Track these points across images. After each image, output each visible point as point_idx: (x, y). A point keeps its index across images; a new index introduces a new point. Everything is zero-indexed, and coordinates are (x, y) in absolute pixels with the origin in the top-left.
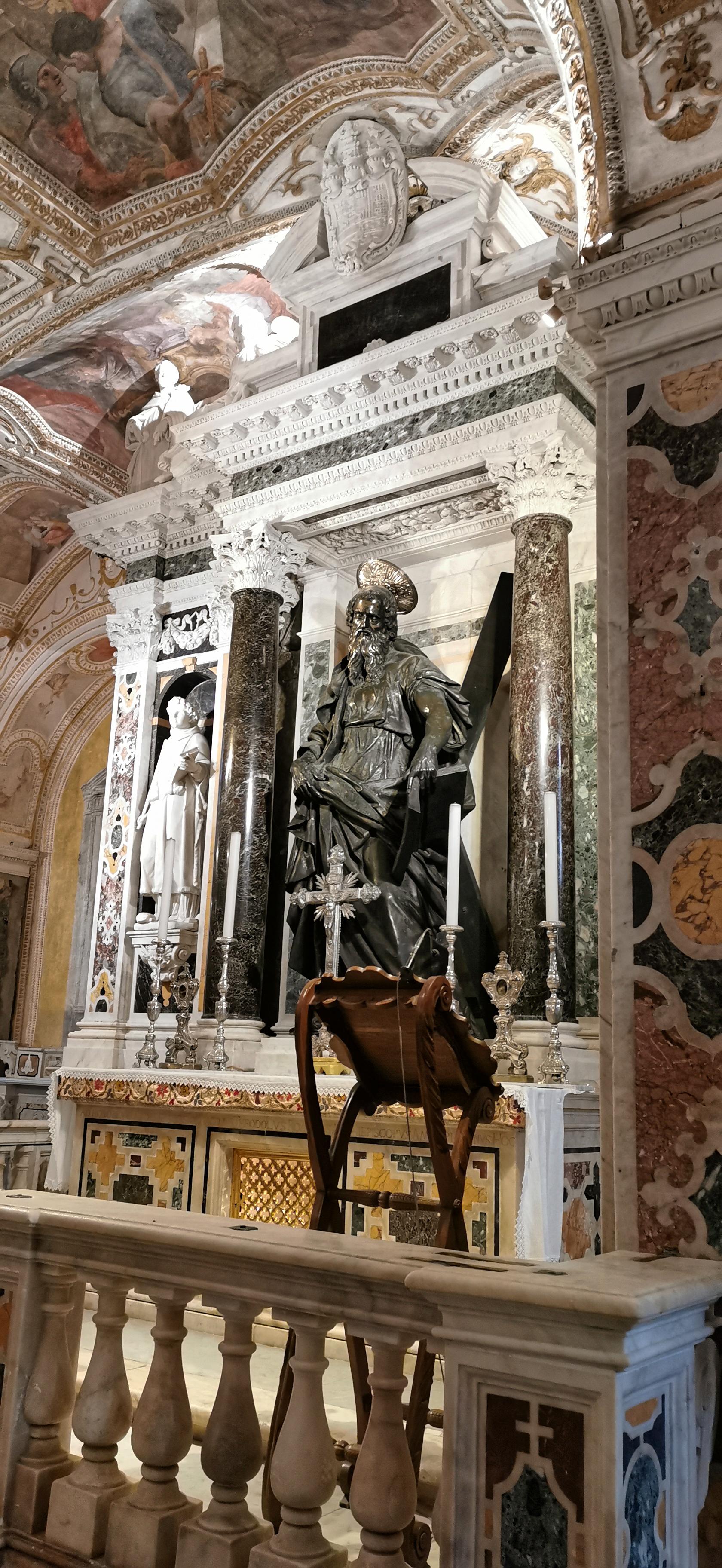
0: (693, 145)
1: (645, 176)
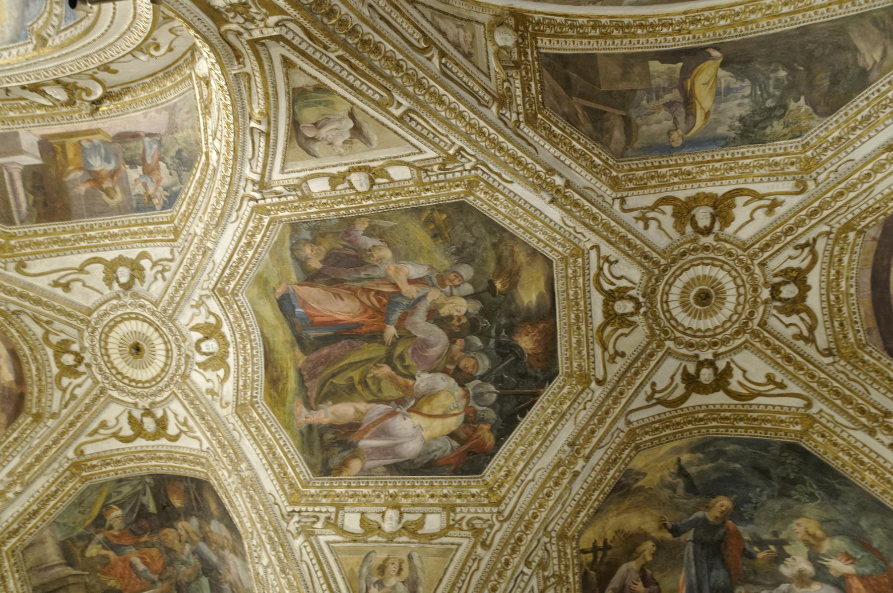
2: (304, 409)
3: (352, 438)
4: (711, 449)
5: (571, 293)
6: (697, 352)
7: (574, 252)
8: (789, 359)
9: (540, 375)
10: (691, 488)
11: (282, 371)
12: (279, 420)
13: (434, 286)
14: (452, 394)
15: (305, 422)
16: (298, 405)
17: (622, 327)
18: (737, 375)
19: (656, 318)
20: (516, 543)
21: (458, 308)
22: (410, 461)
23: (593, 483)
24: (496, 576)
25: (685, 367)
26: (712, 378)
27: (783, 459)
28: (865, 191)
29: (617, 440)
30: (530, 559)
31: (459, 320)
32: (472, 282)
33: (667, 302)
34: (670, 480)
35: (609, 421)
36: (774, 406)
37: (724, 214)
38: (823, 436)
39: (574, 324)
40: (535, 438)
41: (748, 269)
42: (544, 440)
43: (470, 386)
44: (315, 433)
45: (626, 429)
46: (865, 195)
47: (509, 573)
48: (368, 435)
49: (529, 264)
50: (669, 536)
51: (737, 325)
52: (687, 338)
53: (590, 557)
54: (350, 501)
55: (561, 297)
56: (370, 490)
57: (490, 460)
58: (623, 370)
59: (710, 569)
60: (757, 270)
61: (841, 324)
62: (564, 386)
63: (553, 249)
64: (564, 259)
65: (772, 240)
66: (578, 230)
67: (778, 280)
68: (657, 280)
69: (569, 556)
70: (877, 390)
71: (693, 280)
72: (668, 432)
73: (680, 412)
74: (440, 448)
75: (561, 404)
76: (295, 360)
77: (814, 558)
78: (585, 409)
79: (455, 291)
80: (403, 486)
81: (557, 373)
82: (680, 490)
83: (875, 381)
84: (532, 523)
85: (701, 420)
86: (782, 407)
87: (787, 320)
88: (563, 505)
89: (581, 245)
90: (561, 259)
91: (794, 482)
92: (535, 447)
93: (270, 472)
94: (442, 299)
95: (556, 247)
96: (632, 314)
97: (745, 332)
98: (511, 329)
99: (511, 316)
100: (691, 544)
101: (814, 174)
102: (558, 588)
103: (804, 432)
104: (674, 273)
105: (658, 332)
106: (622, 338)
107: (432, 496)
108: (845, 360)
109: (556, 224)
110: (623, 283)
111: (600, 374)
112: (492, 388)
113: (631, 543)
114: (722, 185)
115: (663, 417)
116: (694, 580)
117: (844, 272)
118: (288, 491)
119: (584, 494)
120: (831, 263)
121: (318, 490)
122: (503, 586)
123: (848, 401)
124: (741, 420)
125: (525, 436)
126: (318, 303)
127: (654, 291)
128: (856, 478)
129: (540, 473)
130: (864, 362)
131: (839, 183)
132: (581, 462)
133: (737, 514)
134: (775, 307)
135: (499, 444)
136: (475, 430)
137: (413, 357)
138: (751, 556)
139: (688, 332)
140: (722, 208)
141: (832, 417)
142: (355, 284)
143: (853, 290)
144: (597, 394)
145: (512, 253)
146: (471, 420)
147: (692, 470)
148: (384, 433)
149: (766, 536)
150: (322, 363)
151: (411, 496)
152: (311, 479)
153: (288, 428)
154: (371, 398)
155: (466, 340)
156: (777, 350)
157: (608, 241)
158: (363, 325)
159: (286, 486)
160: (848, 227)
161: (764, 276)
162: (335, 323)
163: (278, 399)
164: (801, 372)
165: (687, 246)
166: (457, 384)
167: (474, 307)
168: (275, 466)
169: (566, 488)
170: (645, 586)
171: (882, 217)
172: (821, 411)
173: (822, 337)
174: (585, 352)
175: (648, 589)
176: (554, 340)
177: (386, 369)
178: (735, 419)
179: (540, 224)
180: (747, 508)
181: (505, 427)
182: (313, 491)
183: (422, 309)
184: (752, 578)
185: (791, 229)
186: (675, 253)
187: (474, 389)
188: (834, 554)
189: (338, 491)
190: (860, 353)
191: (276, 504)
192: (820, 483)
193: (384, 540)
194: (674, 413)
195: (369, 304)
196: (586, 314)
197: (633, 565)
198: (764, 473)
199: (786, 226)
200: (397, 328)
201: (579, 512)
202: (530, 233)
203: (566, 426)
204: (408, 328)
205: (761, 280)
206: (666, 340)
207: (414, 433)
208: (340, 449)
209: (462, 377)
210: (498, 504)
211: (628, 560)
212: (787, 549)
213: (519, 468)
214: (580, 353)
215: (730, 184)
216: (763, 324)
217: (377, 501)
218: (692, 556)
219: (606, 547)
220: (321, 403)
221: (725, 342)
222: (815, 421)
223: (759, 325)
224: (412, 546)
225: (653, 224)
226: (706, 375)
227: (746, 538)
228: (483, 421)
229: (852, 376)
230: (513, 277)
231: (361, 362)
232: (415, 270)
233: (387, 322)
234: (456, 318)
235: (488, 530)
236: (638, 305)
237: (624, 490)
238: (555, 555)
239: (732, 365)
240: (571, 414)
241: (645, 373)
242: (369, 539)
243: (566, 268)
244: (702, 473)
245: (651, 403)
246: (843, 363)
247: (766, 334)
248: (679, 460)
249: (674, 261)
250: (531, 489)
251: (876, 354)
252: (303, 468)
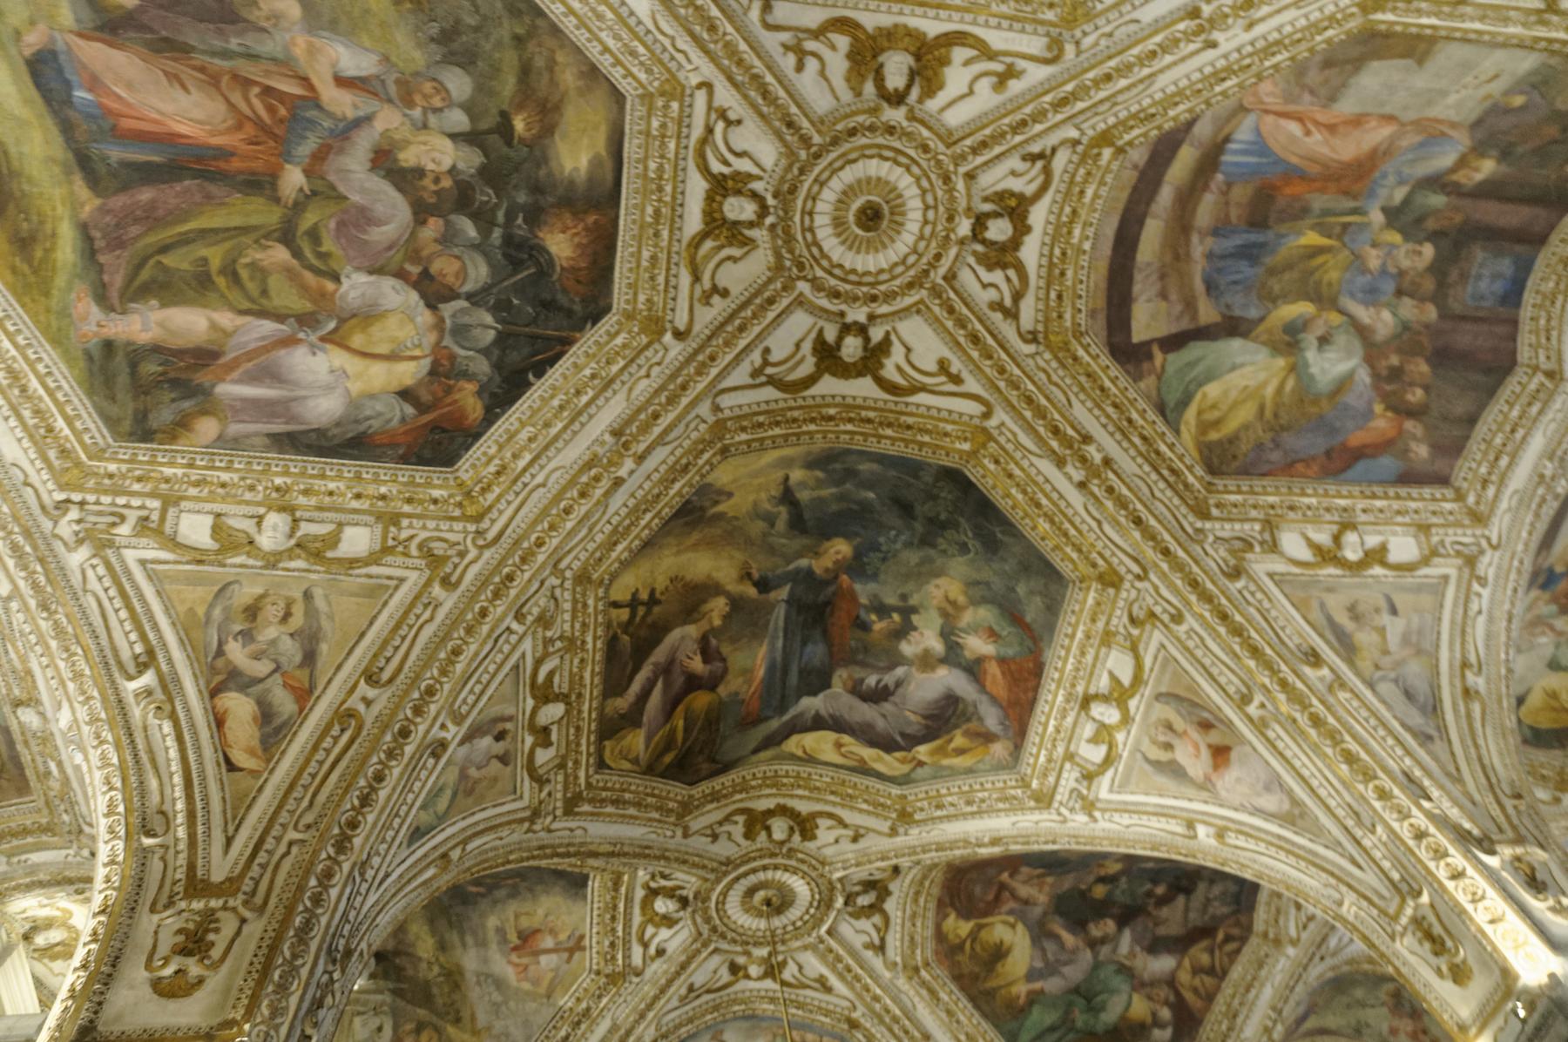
0: (172, 1005)
1: (118, 1018)
2: (95, 312)
3: (203, 378)
4: (838, 466)
5: (652, 165)
6: (843, 307)
7: (667, 87)
8: (975, 339)
9: (577, 308)
10: (798, 523)
11: (42, 223)
12: (37, 322)
13: (390, 101)
14: (412, 320)
15: (96, 334)
16: (79, 299)
17: (731, 245)
18: (897, 352)
19: (789, 239)
20: (502, 582)
21: (436, 155)
22: (320, 432)
23: (645, 500)
24: (462, 632)
25: (821, 331)
26: (859, 353)
27: (935, 491)
28: (1141, 81)
29: (694, 435)
30: (524, 610)
31: (437, 180)
32: (468, 108)
33: (811, 214)
34: (767, 506)
35: (685, 401)
36: (939, 410)
37: (930, 73)
38: (997, 462)
39: (650, 225)
40: (555, 416)
41: (947, 179)
42: (572, 421)
43: (447, 309)
44: (120, 360)
45: (711, 419)
46: (1141, 87)
47: (485, 629)
48: (235, 375)
49: (581, 92)
50: (752, 591)
51: (912, 273)
52: (833, 282)
53: (624, 614)
54: (193, 491)
55: (633, 171)
56: (236, 477)
57: (471, 445)
58: (720, 319)
59: (804, 643)
60: (960, 185)
61: (1060, 297)
62: (617, 333)
63: (629, 74)
64: (647, 97)
65: (992, 137)
66: (681, 44)
67: (988, 207)
68: (802, 171)
69: (591, 610)
70: (1083, 402)
71: (859, 181)
72: (777, 431)
73: (800, 402)
74: (380, 414)
75: (608, 363)
76: (75, 205)
77: (948, 634)
78: (648, 376)
79: (433, 120)
80: (303, 474)
81: (608, 309)
82: (781, 524)
83: (1083, 389)
84: (533, 554)
85: (831, 418)
86: (950, 412)
88: (590, 530)
89: (681, 75)
90: (642, 97)
91: (944, 526)
92: (554, 431)
93: (13, 422)
94: (405, 132)
95: (635, 70)
96: (751, 225)
97: (921, 286)
98: (535, 216)
99: (537, 189)
100: (783, 605)
101: (1078, 33)
102: (567, 657)
103: (974, 453)
104: (830, 164)
105: (788, 263)
106: (729, 264)
107: (358, 496)
108: (1052, 351)
109: (640, 23)
110: (744, 165)
111: (681, 321)
112: (489, 319)
113: (691, 598)
114: (937, 18)
115: (773, 406)
116: (779, 659)
117: (1083, 213)
118: (56, 463)
119: (628, 515)
120: (1068, 193)
121: (124, 467)
122: (473, 648)
123: (1041, 413)
124: (890, 425)
125: (539, 409)
126: (129, 86)
127: (793, 190)
128: (1025, 526)
129: (558, 473)
130: (1075, 359)
131: (1110, 58)
132: (629, 464)
133: (857, 567)
134: (975, 253)
135: (490, 418)
136: (449, 390)
137: (338, 238)
138: (865, 627)
139: (837, 271)
140: (929, 59)
141: (1014, 435)
142: (217, 61)
143: (1087, 246)
144: (672, 354)
145: (551, 65)
146: (443, 371)
147: (804, 496)
148: (269, 374)
149: (891, 600)
150: (136, 221)
151: (317, 493)
152: (109, 446)
153: (56, 342)
154: (246, 305)
155: (448, 223)
156: (961, 323)
157: (730, 79)
158: (233, 154)
159: (52, 454)
160: (1105, 138)
161: (969, 196)
162: (168, 140)
163: (32, 279)
164: (988, 362)
165: (860, 119)
166: (422, 303)
167: (469, 160)
168: (27, 414)
169: (598, 502)
170: (706, 661)
171: (1155, 132)
172: (1003, 424)
173: (1029, 311)
174: (661, 279)
175: (708, 667)
176: (611, 249)
177: (281, 254)
178: (881, 424)
179: (610, 15)
180: (874, 557)
181: (508, 387)
182: (112, 467)
183: (363, 144)
184: (860, 657)
185: (1024, 123)
186: (839, 127)
187: (454, 316)
188: (974, 629)
189: (168, 471)
190: (1075, 345)
191: (27, 484)
192: (979, 533)
193: (259, 564)
194: (793, 404)
195: (248, 112)
196: (673, 210)
197: (692, 631)
198: (906, 509)
199: (1018, 117)
200: (308, 173)
201: (615, 544)
202: (590, 31)
203: (612, 402)
204: (332, 178)
205: (962, 204)
206: (799, 278)
207: (327, 380)
208: (173, 395)
209: (433, 292)
210: (478, 518)
211: (685, 623)
212: (915, 619)
213: (521, 464)
214: (652, 278)
215: (950, 20)
216: (950, 277)
217: (248, 496)
218: (781, 623)
219: (653, 600)
220: (132, 300)
221: (890, 296)
222: (991, 438)
223: (945, 278)
224: (314, 576)
225: (812, 65)
226: (851, 348)
227: (863, 600)
228: (466, 375)
229: (1055, 378)
230: (548, 113)
231: (227, 230)
232: (354, 60)
233: (287, 156)
234: (430, 177)
235: (456, 560)
236: (764, 210)
237: (693, 515)
238: (567, 606)
239: (893, 337)
240: (623, 383)
241: (757, 330)
242: (229, 561)
243: (649, 116)
244: (820, 501)
245: (758, 381)
246: (1047, 356)
247: (952, 295)
248: (787, 478)
249: (835, 142)
250: (538, 499)
251: (1094, 350)
252: (90, 421)
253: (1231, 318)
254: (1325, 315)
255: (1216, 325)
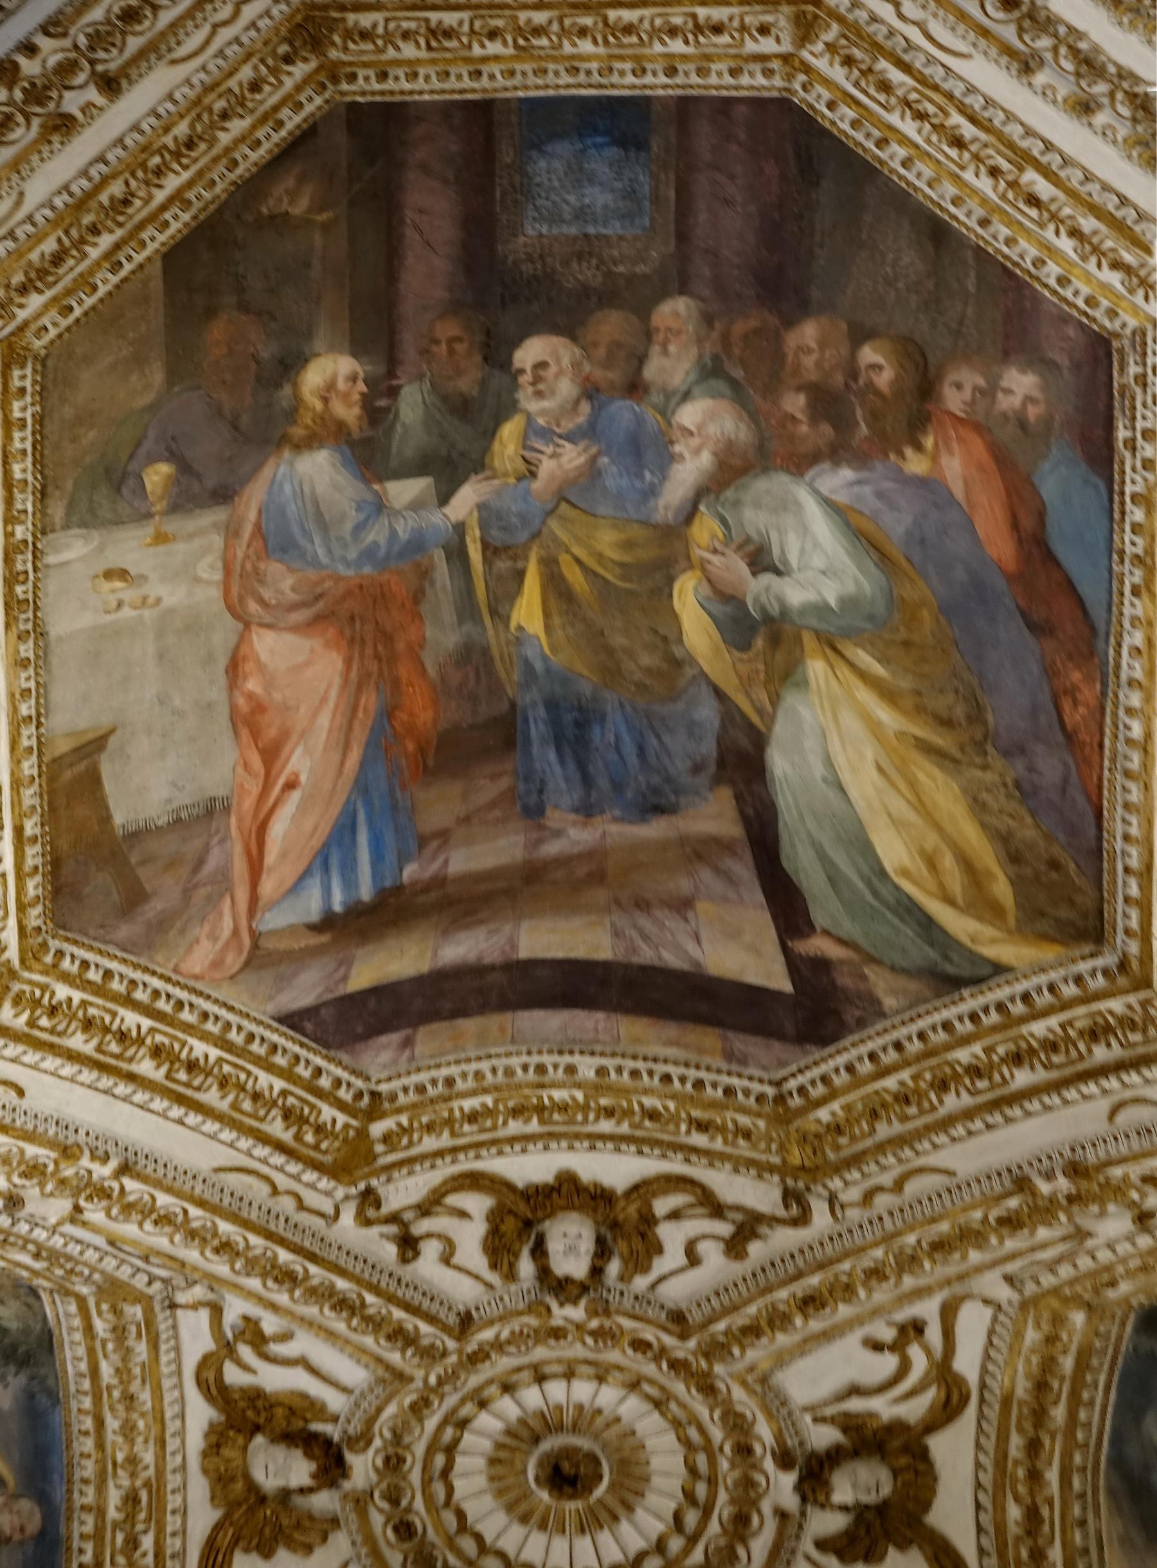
25: (822, 1545)
41: (476, 1358)
51: (679, 1388)
87: (672, 1257)
134: (625, 1277)
165: (377, 1520)
239: (829, 1411)
247: (721, 1326)
253: (721, 763)
254: (697, 553)
255: (739, 798)
